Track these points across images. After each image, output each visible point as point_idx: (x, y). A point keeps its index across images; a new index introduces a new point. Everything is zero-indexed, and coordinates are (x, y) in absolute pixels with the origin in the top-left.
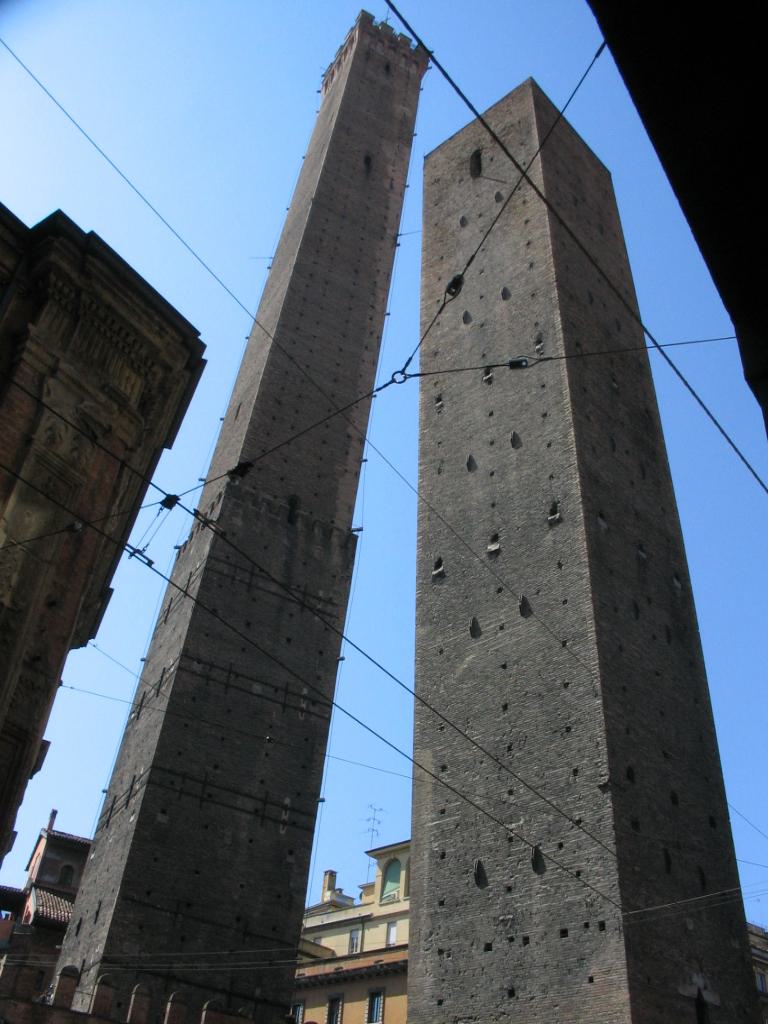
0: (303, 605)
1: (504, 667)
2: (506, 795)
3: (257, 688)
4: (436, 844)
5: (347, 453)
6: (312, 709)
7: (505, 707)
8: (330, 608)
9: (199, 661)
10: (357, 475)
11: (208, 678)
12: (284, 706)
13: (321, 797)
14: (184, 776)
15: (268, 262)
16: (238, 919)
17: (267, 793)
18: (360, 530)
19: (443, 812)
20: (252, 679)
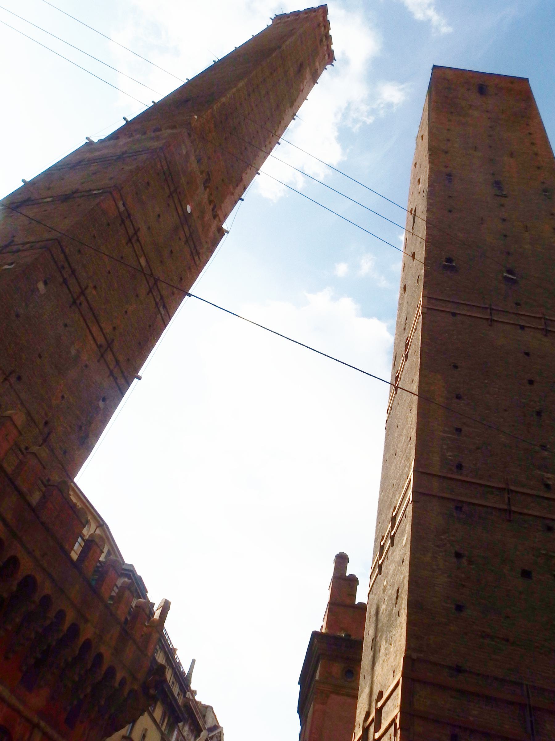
0: (187, 241)
1: (527, 354)
2: (537, 448)
3: (143, 261)
4: (451, 454)
5: (237, 186)
6: (161, 309)
7: (531, 382)
8: (196, 258)
9: (124, 205)
10: (236, 202)
11: (123, 222)
12: (150, 291)
13: (139, 374)
14: (73, 272)
15: (217, 60)
16: (46, 423)
17: (113, 340)
18: (228, 232)
19: (459, 430)
20: (144, 253)
